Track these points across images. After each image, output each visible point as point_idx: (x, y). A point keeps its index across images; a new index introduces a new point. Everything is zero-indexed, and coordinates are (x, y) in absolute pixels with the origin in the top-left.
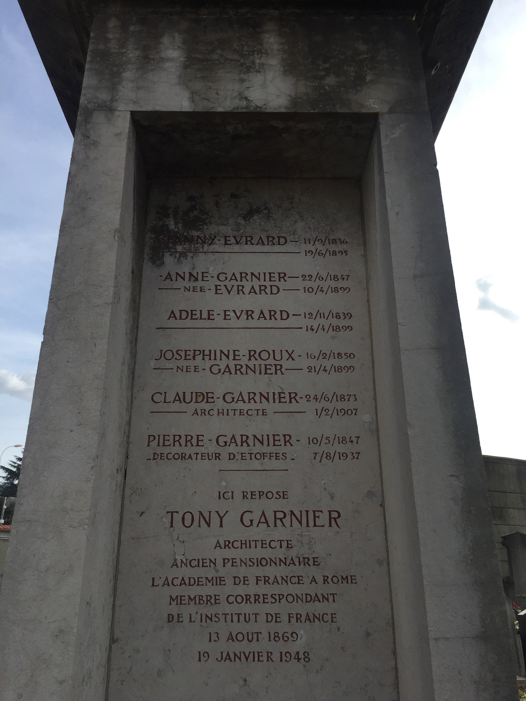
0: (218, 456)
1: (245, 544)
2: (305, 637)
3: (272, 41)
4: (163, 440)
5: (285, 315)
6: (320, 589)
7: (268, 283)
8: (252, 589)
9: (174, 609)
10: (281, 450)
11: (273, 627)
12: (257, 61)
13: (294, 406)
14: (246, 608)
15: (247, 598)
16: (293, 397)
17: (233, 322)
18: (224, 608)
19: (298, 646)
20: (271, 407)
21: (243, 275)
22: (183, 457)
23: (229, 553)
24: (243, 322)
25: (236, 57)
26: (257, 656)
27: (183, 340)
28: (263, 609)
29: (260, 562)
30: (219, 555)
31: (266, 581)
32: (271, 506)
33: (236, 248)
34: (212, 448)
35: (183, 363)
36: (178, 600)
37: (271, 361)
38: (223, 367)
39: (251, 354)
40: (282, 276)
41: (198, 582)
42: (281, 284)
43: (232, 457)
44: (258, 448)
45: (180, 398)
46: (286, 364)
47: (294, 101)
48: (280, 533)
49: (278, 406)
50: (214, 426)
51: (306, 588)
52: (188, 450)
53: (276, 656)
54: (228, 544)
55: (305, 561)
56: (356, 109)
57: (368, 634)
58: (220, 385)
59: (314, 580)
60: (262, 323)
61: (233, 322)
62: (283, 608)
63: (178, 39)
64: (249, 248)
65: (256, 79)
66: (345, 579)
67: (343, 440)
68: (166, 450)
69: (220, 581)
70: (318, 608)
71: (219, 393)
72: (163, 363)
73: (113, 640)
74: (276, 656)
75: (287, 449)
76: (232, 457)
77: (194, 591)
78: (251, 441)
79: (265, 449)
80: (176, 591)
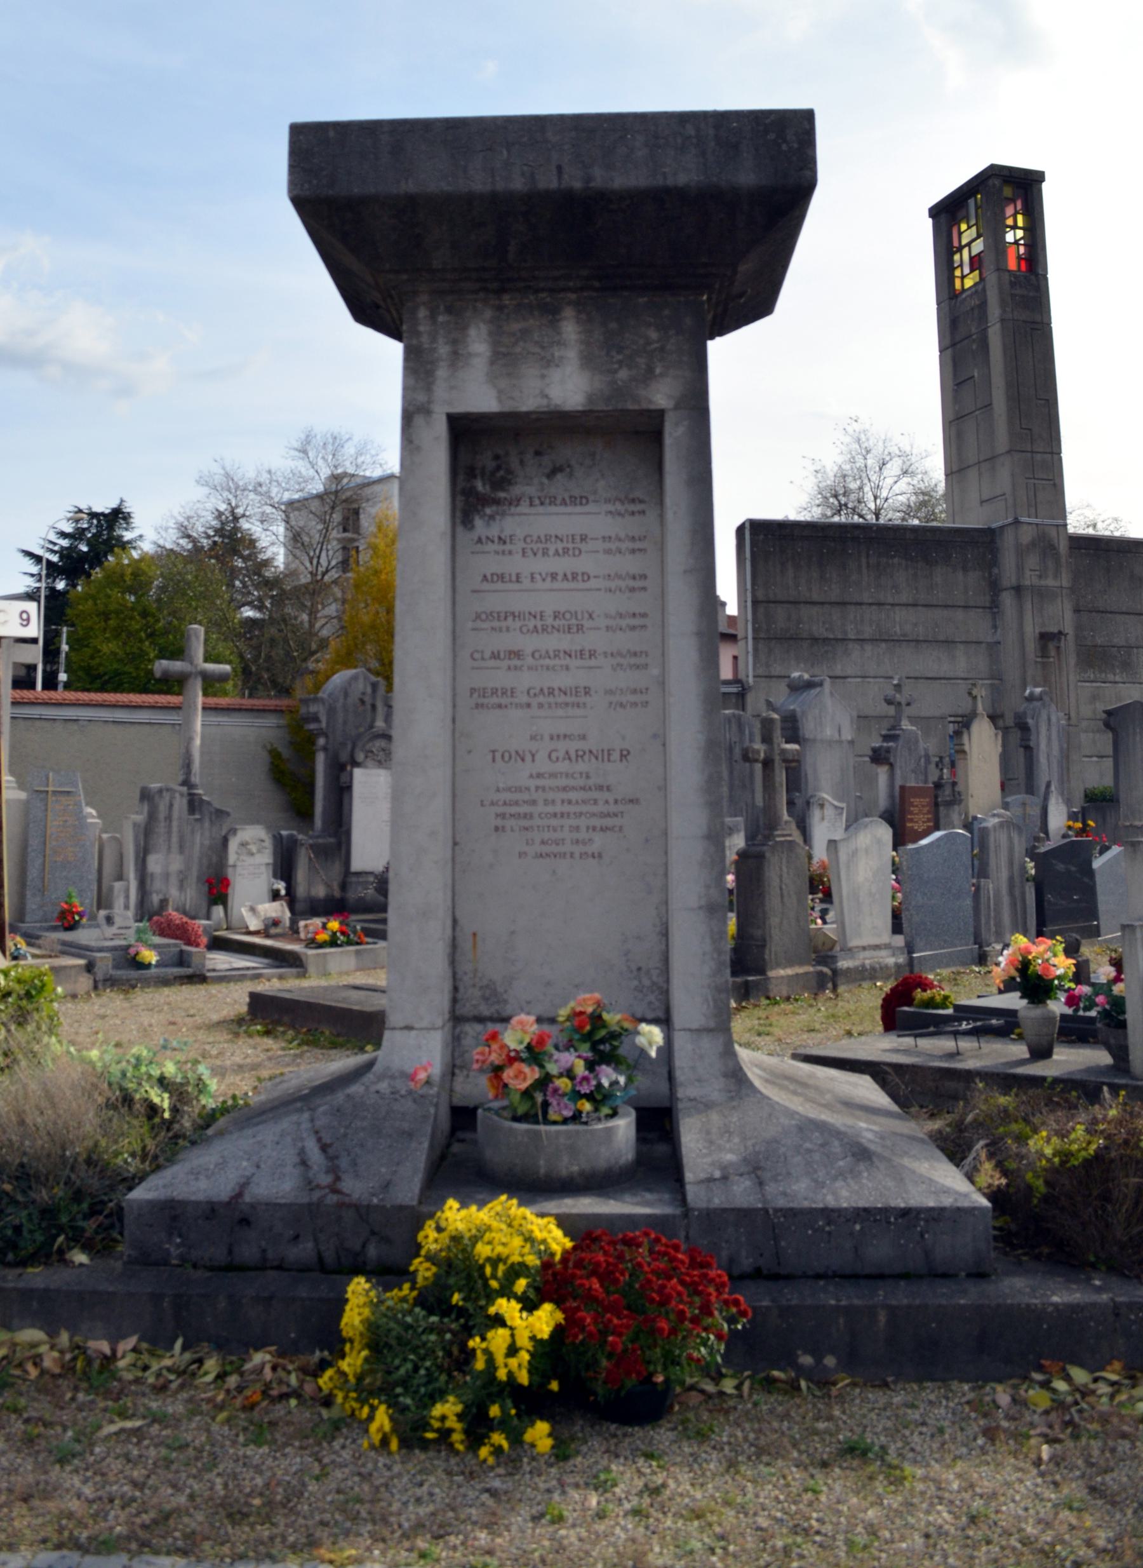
0: (529, 705)
1: (553, 775)
2: (599, 841)
3: (570, 329)
4: (483, 692)
5: (586, 577)
6: (612, 808)
7: (570, 546)
8: (558, 808)
9: (500, 822)
10: (583, 699)
11: (575, 835)
12: (557, 354)
13: (593, 663)
14: (554, 822)
15: (555, 815)
16: (592, 654)
17: (539, 584)
18: (537, 821)
19: (594, 848)
20: (574, 663)
21: (548, 538)
22: (500, 706)
23: (540, 782)
24: (548, 584)
25: (537, 350)
26: (563, 855)
27: (495, 602)
28: (567, 822)
29: (565, 789)
30: (532, 783)
31: (570, 802)
32: (573, 746)
33: (541, 509)
34: (525, 699)
35: (496, 624)
36: (503, 816)
37: (574, 621)
38: (531, 626)
39: (556, 615)
40: (584, 538)
41: (517, 803)
42: (583, 546)
43: (541, 706)
44: (562, 699)
45: (495, 656)
46: (587, 624)
47: (590, 398)
48: (581, 766)
49: (579, 662)
50: (526, 680)
51: (601, 808)
52: (504, 701)
53: (577, 855)
54: (539, 776)
55: (600, 788)
56: (644, 406)
57: (647, 841)
58: (529, 643)
59: (607, 802)
60: (566, 585)
61: (539, 584)
62: (583, 822)
63: (484, 329)
64: (553, 509)
65: (555, 374)
66: (631, 801)
67: (634, 691)
68: (485, 701)
69: (534, 802)
70: (609, 822)
71: (528, 651)
72: (479, 624)
73: (455, 844)
74: (577, 855)
75: (587, 699)
76: (541, 706)
77: (514, 810)
78: (556, 692)
79: (569, 699)
80: (500, 810)
